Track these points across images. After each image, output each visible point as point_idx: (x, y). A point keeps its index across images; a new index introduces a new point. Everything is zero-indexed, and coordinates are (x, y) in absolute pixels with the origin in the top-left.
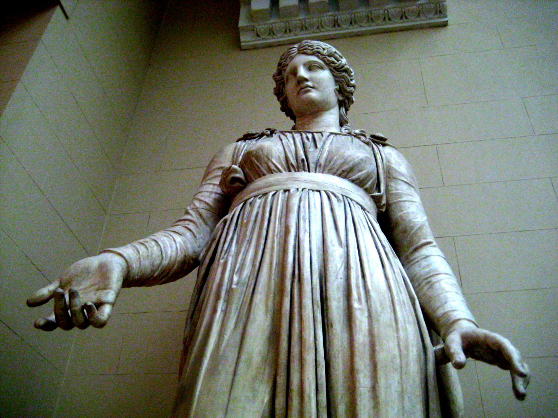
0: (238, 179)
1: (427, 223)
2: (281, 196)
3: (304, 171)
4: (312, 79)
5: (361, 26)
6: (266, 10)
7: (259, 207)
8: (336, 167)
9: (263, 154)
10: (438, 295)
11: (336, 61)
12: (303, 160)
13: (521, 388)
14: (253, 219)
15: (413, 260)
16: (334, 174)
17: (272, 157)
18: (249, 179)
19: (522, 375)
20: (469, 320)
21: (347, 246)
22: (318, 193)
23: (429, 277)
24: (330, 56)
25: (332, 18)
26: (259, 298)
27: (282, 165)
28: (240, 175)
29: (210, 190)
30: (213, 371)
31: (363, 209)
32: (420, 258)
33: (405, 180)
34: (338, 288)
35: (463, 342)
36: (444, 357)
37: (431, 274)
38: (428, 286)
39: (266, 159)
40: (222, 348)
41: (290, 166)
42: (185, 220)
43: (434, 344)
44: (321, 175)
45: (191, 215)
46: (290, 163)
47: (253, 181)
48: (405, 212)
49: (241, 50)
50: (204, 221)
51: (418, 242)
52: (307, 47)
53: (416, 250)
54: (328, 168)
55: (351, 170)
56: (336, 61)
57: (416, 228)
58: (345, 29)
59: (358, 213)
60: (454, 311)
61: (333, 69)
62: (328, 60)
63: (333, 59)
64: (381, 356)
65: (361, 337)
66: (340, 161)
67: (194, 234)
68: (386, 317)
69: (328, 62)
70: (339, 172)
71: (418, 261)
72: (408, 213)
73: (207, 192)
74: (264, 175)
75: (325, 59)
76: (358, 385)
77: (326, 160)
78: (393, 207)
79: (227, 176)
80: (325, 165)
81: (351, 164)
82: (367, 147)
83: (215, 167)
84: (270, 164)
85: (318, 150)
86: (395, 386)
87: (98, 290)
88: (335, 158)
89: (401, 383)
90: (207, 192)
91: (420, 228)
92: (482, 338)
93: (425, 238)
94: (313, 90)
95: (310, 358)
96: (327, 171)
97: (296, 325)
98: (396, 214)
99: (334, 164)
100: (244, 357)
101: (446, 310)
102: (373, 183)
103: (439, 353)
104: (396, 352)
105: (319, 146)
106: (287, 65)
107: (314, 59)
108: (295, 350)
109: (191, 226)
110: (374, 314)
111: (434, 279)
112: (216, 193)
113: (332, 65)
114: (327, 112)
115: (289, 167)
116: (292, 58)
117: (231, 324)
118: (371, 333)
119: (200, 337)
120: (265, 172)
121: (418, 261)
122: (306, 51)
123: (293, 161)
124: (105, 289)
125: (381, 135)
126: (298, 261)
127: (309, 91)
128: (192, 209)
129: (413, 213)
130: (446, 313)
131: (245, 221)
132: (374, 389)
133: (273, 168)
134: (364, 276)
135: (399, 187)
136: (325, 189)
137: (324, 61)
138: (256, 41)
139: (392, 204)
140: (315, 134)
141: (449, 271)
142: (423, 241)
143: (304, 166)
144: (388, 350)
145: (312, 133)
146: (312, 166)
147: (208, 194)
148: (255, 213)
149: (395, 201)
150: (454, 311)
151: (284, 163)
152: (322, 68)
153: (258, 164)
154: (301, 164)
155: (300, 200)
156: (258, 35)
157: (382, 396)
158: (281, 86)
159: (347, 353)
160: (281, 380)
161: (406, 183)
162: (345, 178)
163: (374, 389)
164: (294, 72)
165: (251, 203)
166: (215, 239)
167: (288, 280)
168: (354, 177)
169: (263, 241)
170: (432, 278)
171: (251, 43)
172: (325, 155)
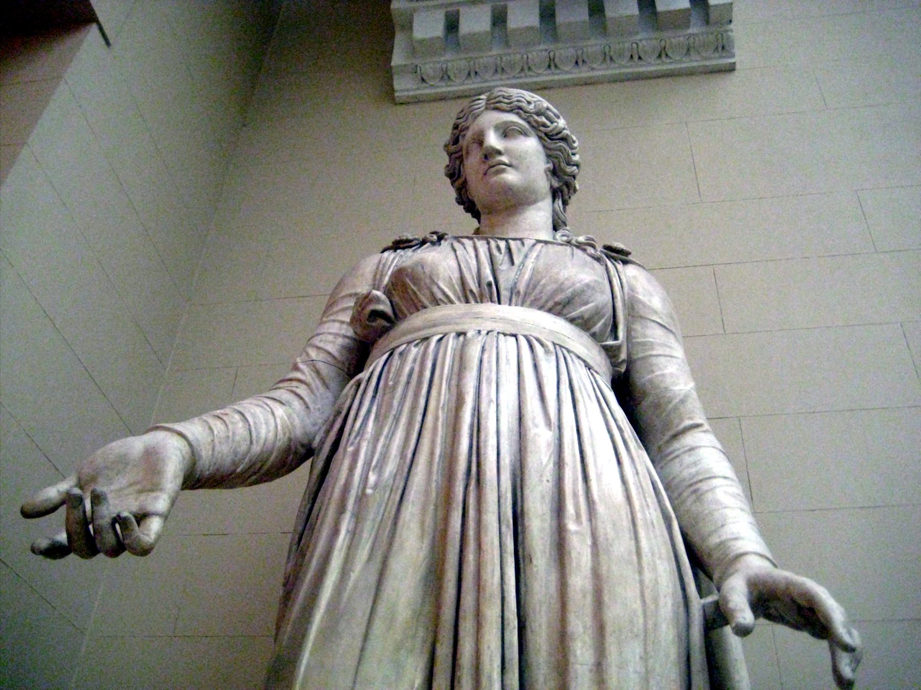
0: (381, 315)
1: (694, 395)
3: (492, 301)
4: (508, 152)
5: (593, 69)
6: (439, 38)
7: (415, 360)
8: (544, 298)
9: (424, 273)
10: (711, 513)
11: (548, 123)
12: (489, 285)
13: (846, 671)
14: (404, 379)
15: (671, 453)
16: (541, 308)
17: (438, 275)
18: (400, 315)
19: (848, 649)
20: (761, 556)
21: (560, 428)
22: (513, 339)
23: (696, 483)
24: (539, 114)
25: (545, 54)
26: (411, 511)
27: (455, 293)
28: (385, 307)
29: (334, 331)
30: (330, 631)
31: (588, 367)
32: (682, 450)
33: (659, 321)
34: (543, 497)
35: (751, 593)
36: (717, 618)
37: (700, 478)
38: (694, 497)
39: (428, 281)
40: (346, 595)
41: (468, 293)
42: (291, 380)
43: (701, 593)
44: (519, 308)
46: (467, 288)
47: (405, 316)
48: (658, 373)
49: (396, 104)
51: (679, 424)
52: (501, 99)
53: (675, 436)
56: (548, 123)
58: (568, 72)
59: (580, 374)
60: (736, 539)
61: (543, 135)
62: (536, 121)
63: (544, 119)
64: (613, 613)
65: (580, 581)
66: (550, 288)
67: (305, 403)
68: (622, 546)
69: (534, 124)
70: (550, 304)
71: (677, 456)
72: (663, 375)
73: (330, 333)
74: (425, 307)
75: (531, 119)
76: (572, 659)
77: (528, 286)
78: (638, 364)
79: (363, 309)
81: (569, 292)
82: (596, 265)
83: (343, 294)
84: (435, 290)
85: (515, 268)
86: (634, 666)
87: (140, 492)
88: (543, 282)
89: (645, 658)
90: (330, 333)
91: (683, 401)
92: (782, 586)
93: (691, 418)
94: (509, 168)
95: (492, 613)
96: (528, 302)
97: (470, 557)
98: (642, 378)
99: (541, 292)
100: (382, 609)
101: (723, 538)
102: (605, 325)
103: (710, 611)
104: (637, 606)
105: (517, 261)
106: (467, 128)
109: (302, 390)
111: (704, 486)
112: (345, 336)
113: (542, 128)
114: (532, 207)
115: (466, 296)
116: (476, 117)
117: (363, 554)
120: (426, 302)
121: (677, 456)
123: (473, 285)
124: (152, 490)
125: (620, 245)
126: (476, 450)
127: (503, 171)
128: (304, 362)
129: (672, 375)
130: (722, 543)
131: (391, 383)
133: (439, 295)
135: (649, 332)
136: (526, 333)
137: (529, 123)
138: (418, 89)
139: (639, 359)
140: (511, 242)
141: (730, 473)
142: (687, 423)
144: (624, 603)
145: (507, 240)
146: (505, 294)
147: (330, 338)
149: (641, 355)
150: (736, 539)
151: (458, 288)
152: (524, 134)
153: (415, 289)
155: (483, 350)
156: (423, 80)
158: (458, 162)
159: (557, 606)
160: (444, 651)
161: (661, 325)
162: (559, 314)
164: (480, 140)
165: (401, 354)
168: (574, 314)
169: (419, 418)
170: (699, 485)
171: (411, 93)
172: (527, 277)
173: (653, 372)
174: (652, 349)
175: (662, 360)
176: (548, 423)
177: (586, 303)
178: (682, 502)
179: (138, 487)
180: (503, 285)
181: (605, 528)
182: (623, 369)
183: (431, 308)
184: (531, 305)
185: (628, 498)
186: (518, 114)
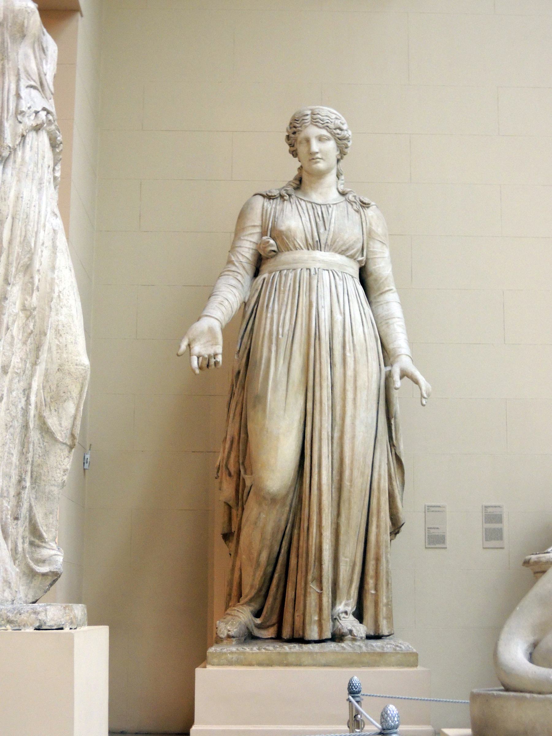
0: (274, 251)
2: (306, 274)
4: (321, 151)
7: (291, 279)
8: (338, 248)
12: (317, 242)
13: (424, 402)
14: (287, 289)
15: (378, 302)
16: (336, 252)
19: (425, 398)
20: (407, 355)
21: (344, 314)
22: (327, 272)
27: (303, 245)
28: (275, 248)
31: (353, 277)
39: (293, 239)
40: (278, 376)
43: (385, 366)
45: (236, 266)
48: (377, 266)
50: (247, 272)
53: (381, 294)
54: (333, 248)
55: (347, 249)
57: (383, 279)
59: (349, 279)
60: (399, 348)
62: (335, 133)
63: (338, 131)
64: (360, 383)
66: (341, 243)
67: (242, 284)
68: (362, 359)
70: (340, 250)
71: (382, 304)
74: (291, 250)
76: (347, 397)
78: (370, 261)
79: (265, 247)
80: (331, 245)
81: (347, 246)
82: (357, 214)
84: (296, 243)
85: (327, 232)
87: (212, 345)
88: (338, 240)
91: (386, 279)
93: (388, 286)
94: (321, 160)
95: (325, 385)
97: (318, 366)
98: (372, 267)
100: (291, 381)
101: (395, 346)
103: (388, 373)
104: (366, 379)
106: (301, 131)
107: (324, 132)
108: (317, 380)
109: (239, 278)
110: (357, 359)
112: (252, 249)
113: (338, 136)
115: (308, 247)
116: (306, 127)
117: (281, 361)
118: (355, 370)
119: (263, 366)
120: (291, 247)
121: (382, 304)
122: (317, 124)
123: (310, 241)
124: (216, 345)
125: (366, 200)
126: (318, 326)
127: (318, 162)
128: (237, 261)
131: (282, 289)
132: (355, 399)
133: (297, 246)
134: (352, 335)
136: (332, 269)
140: (322, 206)
142: (387, 288)
143: (318, 247)
146: (323, 246)
148: (288, 284)
149: (372, 257)
150: (399, 348)
151: (304, 242)
152: (329, 139)
154: (316, 246)
155: (318, 281)
157: (358, 404)
160: (310, 395)
162: (342, 254)
163: (355, 399)
164: (308, 141)
166: (257, 290)
167: (313, 339)
168: (349, 254)
169: (295, 308)
172: (331, 237)
173: (375, 265)
174: (376, 254)
175: (380, 260)
176: (341, 313)
177: (353, 249)
178: (381, 326)
179: (210, 343)
180: (323, 242)
181: (358, 355)
182: (363, 265)
183: (295, 251)
184: (333, 251)
185: (365, 340)
186: (327, 130)
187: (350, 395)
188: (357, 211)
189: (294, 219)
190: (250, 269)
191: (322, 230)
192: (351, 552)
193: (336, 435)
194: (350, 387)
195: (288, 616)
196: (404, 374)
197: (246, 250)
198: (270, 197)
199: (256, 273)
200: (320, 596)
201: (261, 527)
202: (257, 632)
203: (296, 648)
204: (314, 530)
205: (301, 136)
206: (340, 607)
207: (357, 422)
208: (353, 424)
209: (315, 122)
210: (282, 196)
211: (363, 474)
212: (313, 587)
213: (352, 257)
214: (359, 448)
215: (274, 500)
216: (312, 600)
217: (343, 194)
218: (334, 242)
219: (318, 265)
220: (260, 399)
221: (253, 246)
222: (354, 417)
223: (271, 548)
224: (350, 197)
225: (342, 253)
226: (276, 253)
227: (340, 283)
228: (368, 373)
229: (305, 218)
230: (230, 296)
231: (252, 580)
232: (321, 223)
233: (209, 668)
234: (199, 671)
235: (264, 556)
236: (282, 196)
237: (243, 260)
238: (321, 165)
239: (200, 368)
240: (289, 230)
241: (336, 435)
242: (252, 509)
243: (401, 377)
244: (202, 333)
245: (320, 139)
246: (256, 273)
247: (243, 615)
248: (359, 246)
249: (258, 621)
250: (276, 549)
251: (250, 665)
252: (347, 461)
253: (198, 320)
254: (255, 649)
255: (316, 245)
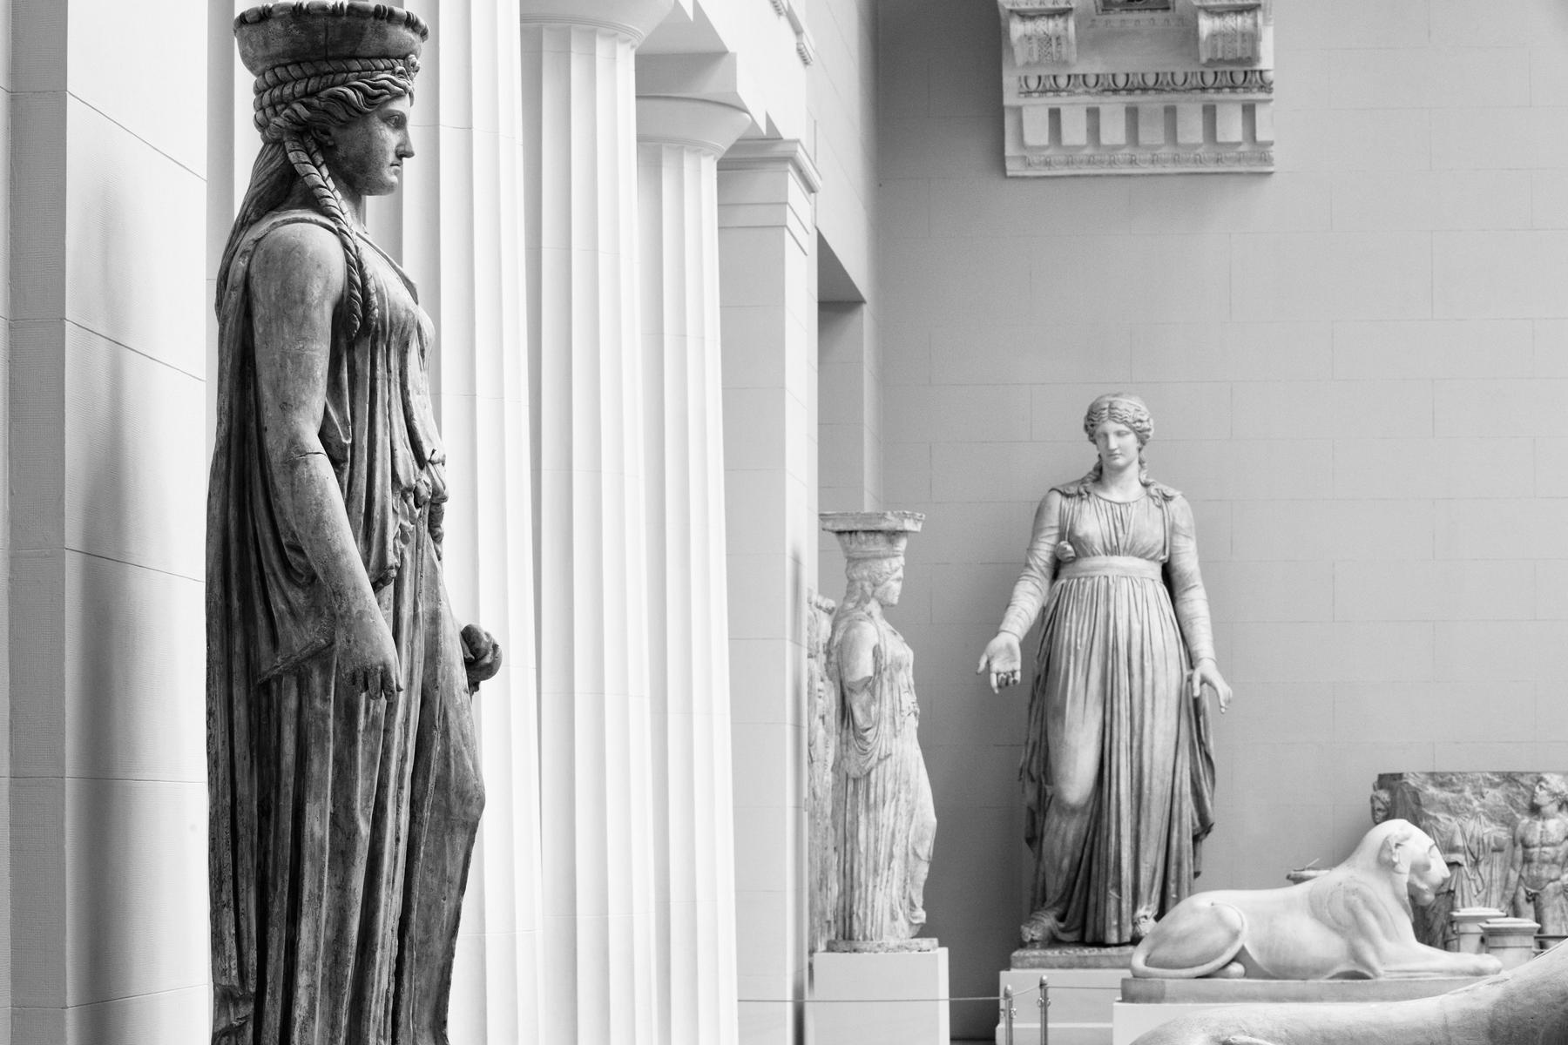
30: (1074, 700)
64: (1158, 693)
65: (1148, 683)
98: (1175, 563)
107: (1122, 427)
115: (1106, 552)
126: (1115, 637)
164: (1106, 435)
167: (1110, 651)
181: (1157, 664)
187: (1148, 705)
188: (1160, 507)
189: (1092, 523)
190: (1048, 572)
191: (1120, 534)
192: (1151, 857)
193: (1135, 744)
194: (1148, 697)
195: (1090, 921)
196: (1203, 681)
197: (1043, 553)
198: (1068, 496)
199: (1055, 576)
200: (1119, 902)
201: (1064, 834)
202: (1061, 936)
203: (1095, 951)
204: (1113, 838)
205: (1099, 430)
206: (1141, 912)
207: (1156, 732)
208: (1152, 733)
209: (1112, 417)
210: (1080, 494)
211: (1162, 782)
212: (1113, 893)
213: (1152, 559)
214: (1158, 756)
215: (1073, 811)
216: (1112, 906)
217: (1145, 485)
218: (1133, 545)
219: (1117, 572)
220: (1060, 712)
221: (1049, 548)
222: (1152, 727)
223: (1073, 855)
224: (1152, 490)
225: (1141, 556)
226: (1074, 559)
227: (1138, 590)
228: (1166, 677)
229: (1104, 520)
230: (1027, 602)
231: (1055, 885)
232: (1119, 525)
233: (1013, 971)
234: (1003, 974)
235: (1066, 863)
236: (1080, 494)
237: (1041, 564)
238: (1120, 461)
239: (999, 686)
240: (1087, 536)
241: (1135, 744)
242: (1053, 820)
243: (1202, 683)
244: (1000, 650)
245: (1119, 434)
246: (1055, 576)
247: (1048, 921)
248: (1160, 546)
249: (1062, 925)
250: (1078, 854)
251: (1052, 967)
252: (1146, 770)
253: (996, 634)
254: (1056, 952)
255: (1113, 550)
